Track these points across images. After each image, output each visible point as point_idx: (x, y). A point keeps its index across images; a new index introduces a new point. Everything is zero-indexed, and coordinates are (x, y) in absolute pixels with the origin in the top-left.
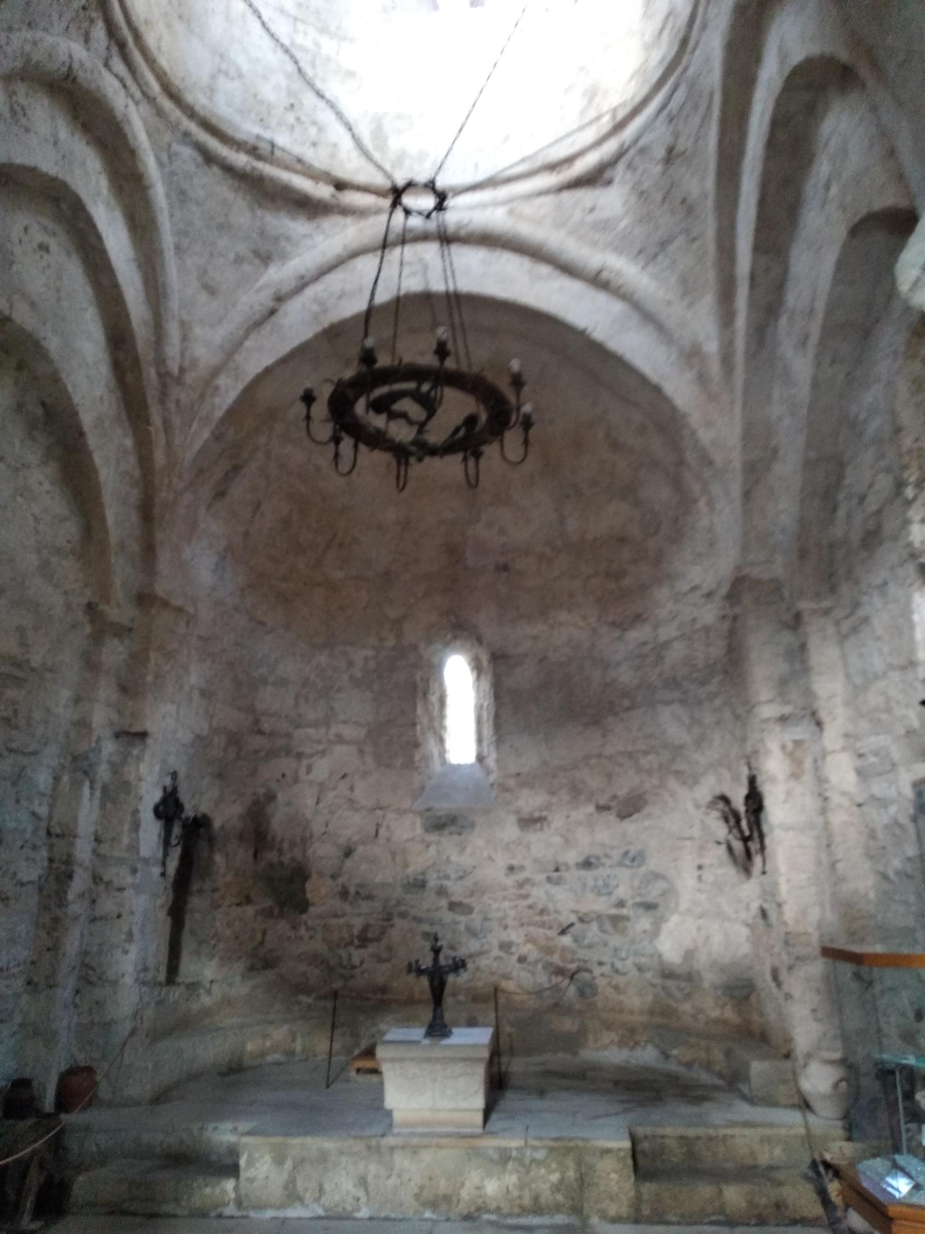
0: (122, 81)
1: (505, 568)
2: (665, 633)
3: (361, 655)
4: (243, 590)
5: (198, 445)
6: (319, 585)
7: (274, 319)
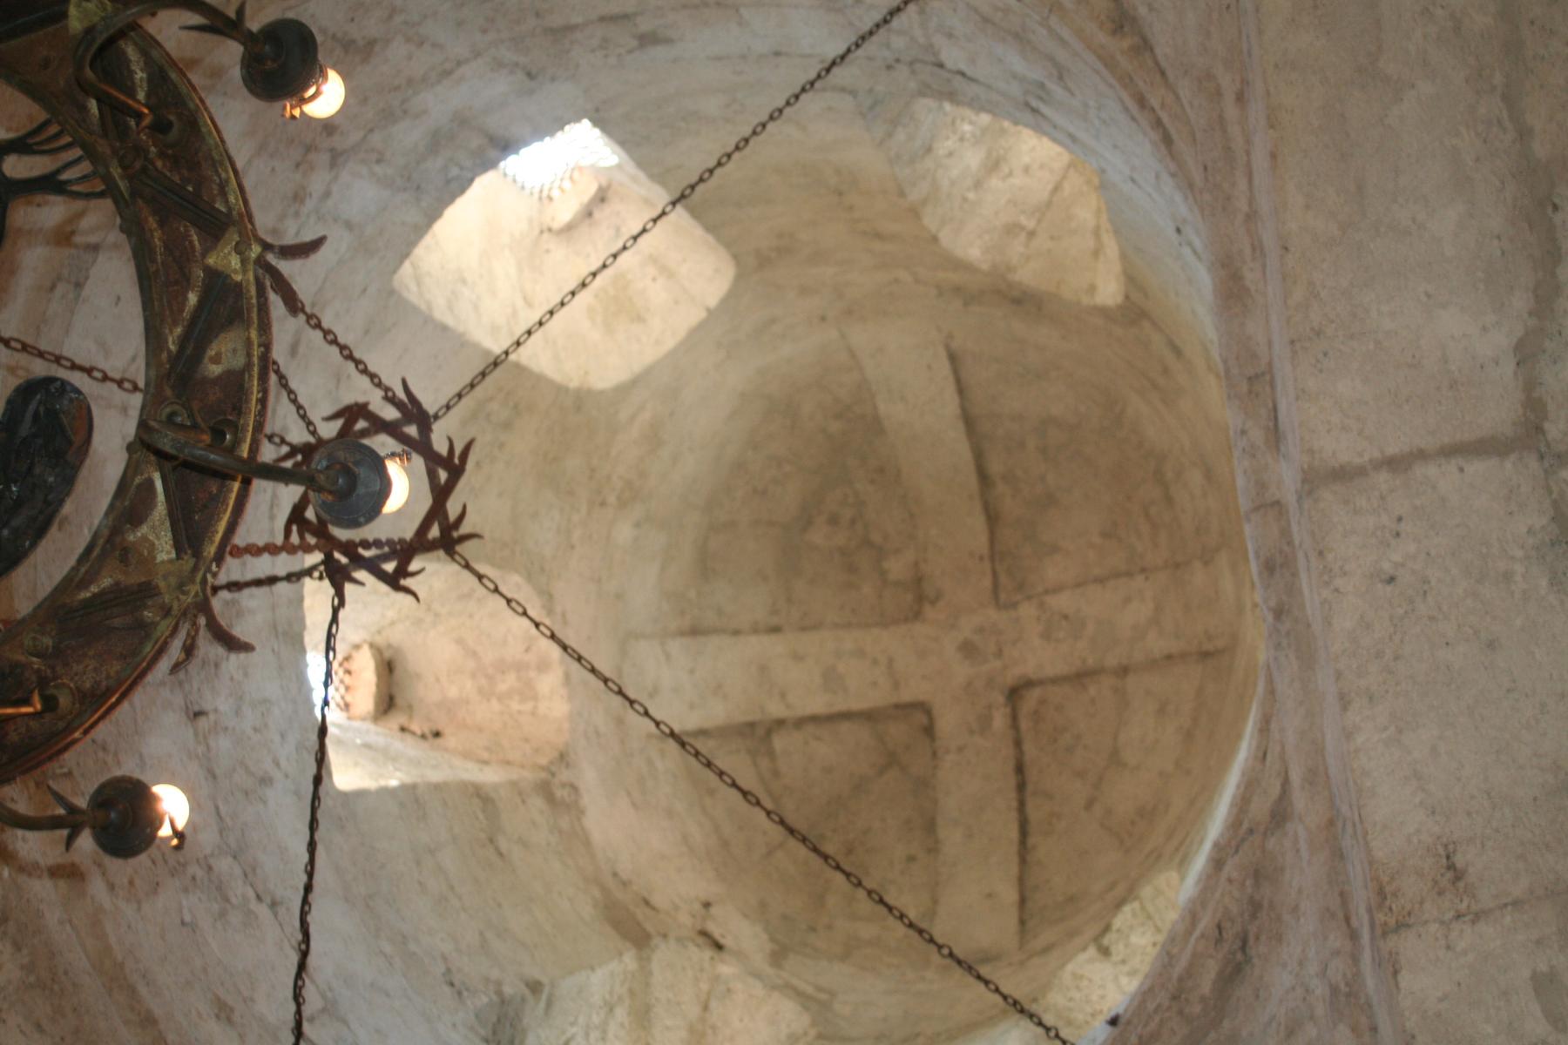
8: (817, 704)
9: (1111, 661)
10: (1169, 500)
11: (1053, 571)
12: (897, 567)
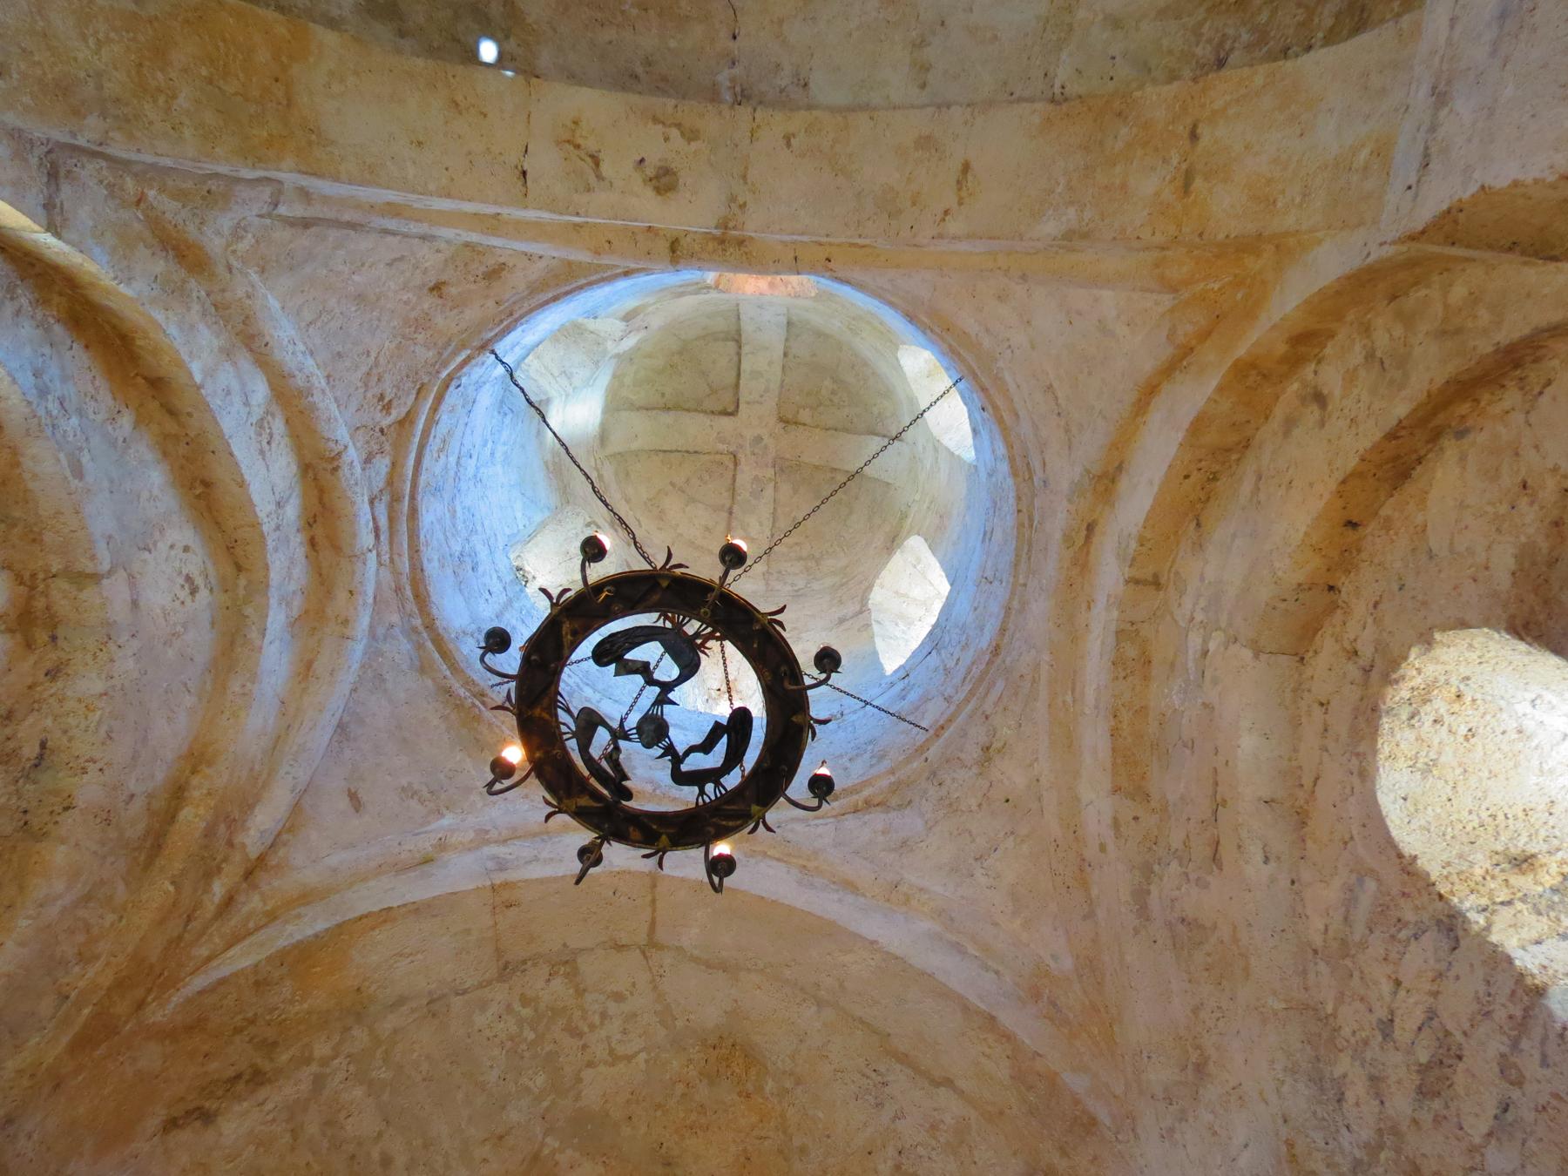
0: (377, 529)
7: (426, 868)
8: (745, 366)
9: (736, 508)
10: (800, 558)
11: (785, 488)
12: (805, 416)
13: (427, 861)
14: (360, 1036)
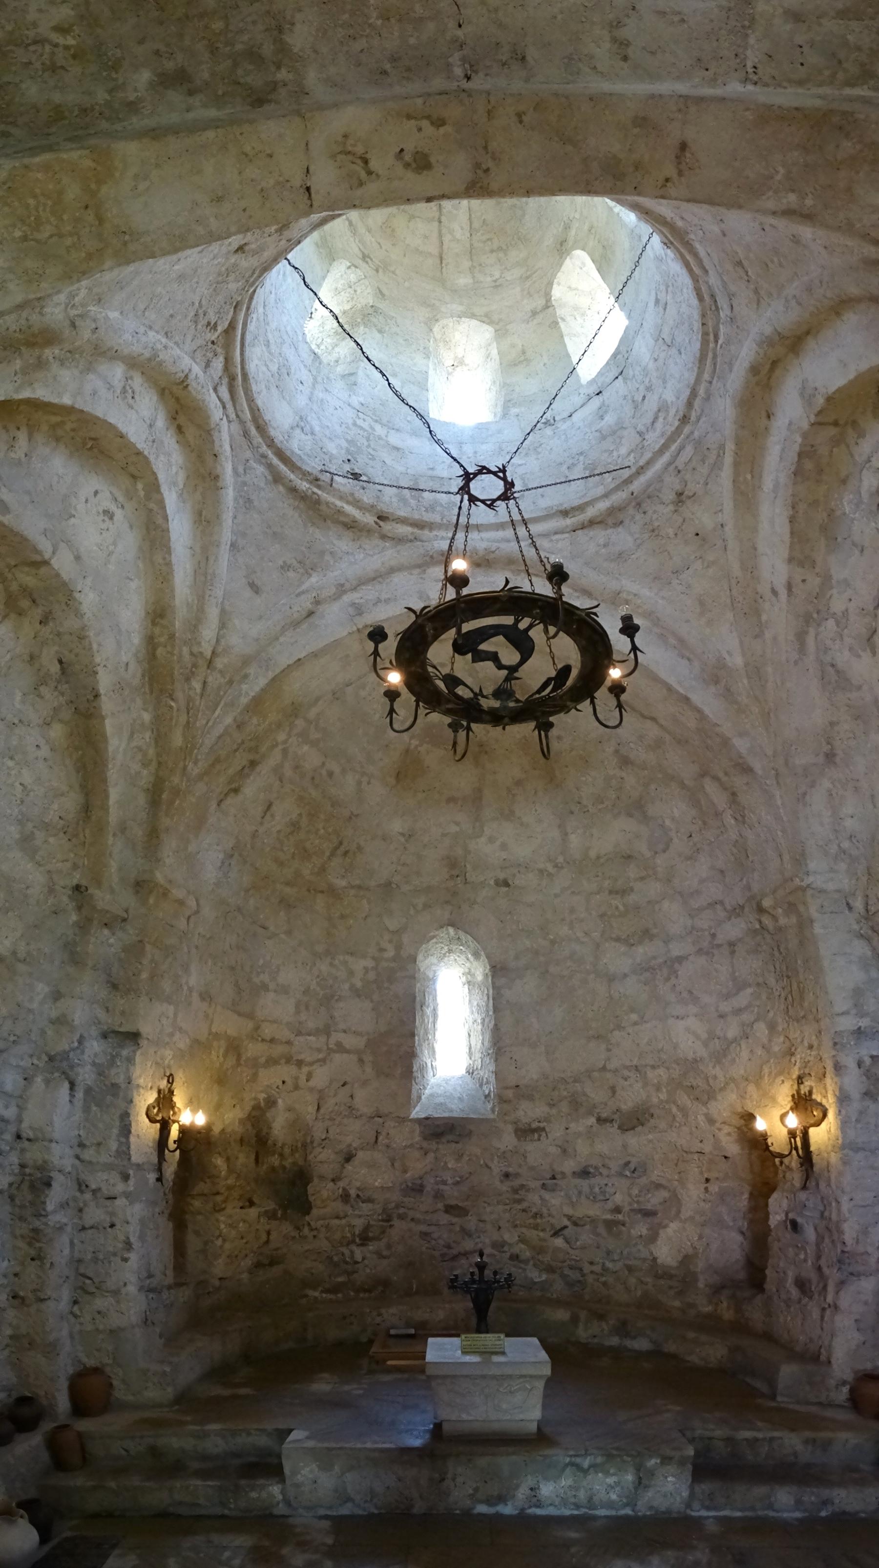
1: (506, 884)
2: (676, 950)
3: (359, 965)
4: (247, 891)
5: (219, 730)
6: (322, 892)
7: (311, 620)
13: (311, 614)
14: (300, 723)
